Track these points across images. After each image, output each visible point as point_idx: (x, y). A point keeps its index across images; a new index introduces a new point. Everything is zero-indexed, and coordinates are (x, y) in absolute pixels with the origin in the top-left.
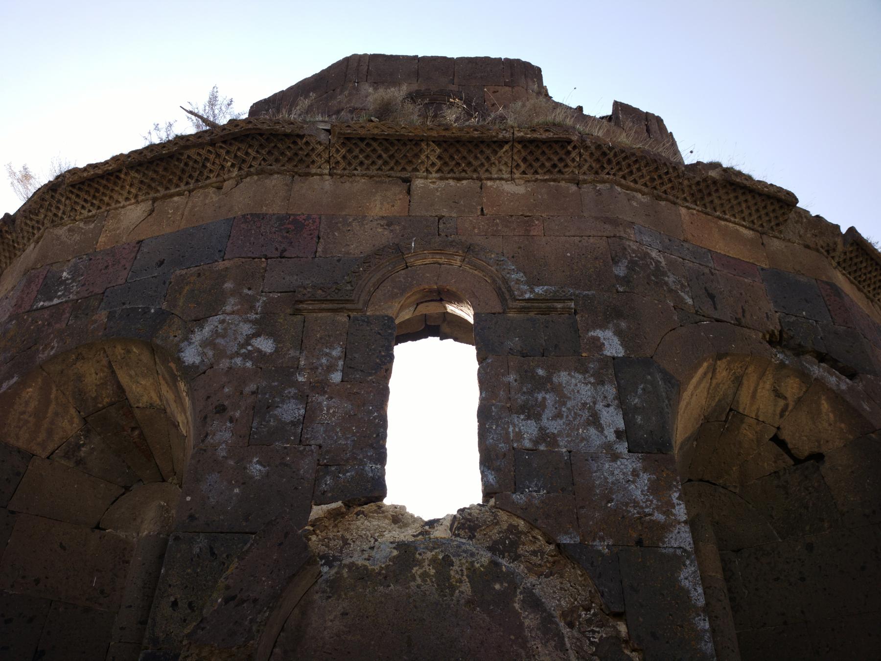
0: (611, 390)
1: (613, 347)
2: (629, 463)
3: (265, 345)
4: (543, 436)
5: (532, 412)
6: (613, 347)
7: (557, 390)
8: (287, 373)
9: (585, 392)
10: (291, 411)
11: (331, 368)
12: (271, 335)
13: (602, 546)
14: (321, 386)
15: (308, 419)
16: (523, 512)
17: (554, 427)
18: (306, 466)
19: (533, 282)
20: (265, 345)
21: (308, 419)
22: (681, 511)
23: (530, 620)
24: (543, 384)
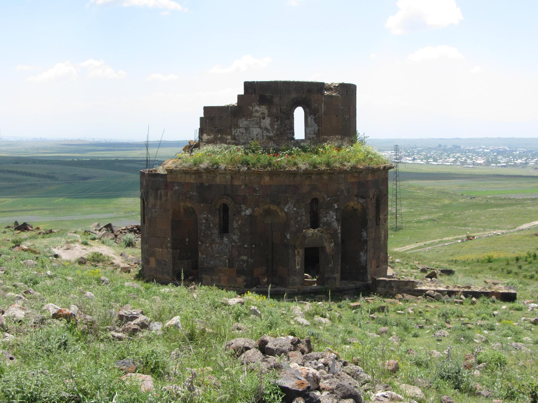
0: (335, 213)
1: (336, 207)
2: (336, 222)
3: (295, 209)
4: (327, 220)
5: (326, 217)
6: (336, 207)
7: (329, 214)
8: (298, 213)
9: (332, 214)
10: (299, 219)
11: (303, 212)
12: (296, 207)
13: (332, 232)
14: (302, 215)
15: (302, 220)
16: (325, 229)
17: (328, 218)
18: (302, 226)
19: (328, 198)
20: (295, 209)
21: (302, 220)
22: (340, 228)
23: (324, 240)
24: (328, 213)
